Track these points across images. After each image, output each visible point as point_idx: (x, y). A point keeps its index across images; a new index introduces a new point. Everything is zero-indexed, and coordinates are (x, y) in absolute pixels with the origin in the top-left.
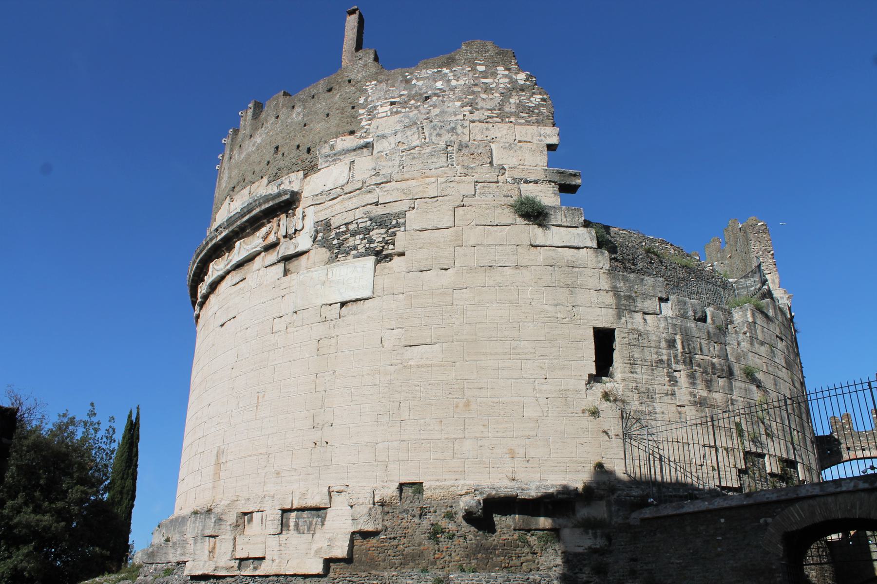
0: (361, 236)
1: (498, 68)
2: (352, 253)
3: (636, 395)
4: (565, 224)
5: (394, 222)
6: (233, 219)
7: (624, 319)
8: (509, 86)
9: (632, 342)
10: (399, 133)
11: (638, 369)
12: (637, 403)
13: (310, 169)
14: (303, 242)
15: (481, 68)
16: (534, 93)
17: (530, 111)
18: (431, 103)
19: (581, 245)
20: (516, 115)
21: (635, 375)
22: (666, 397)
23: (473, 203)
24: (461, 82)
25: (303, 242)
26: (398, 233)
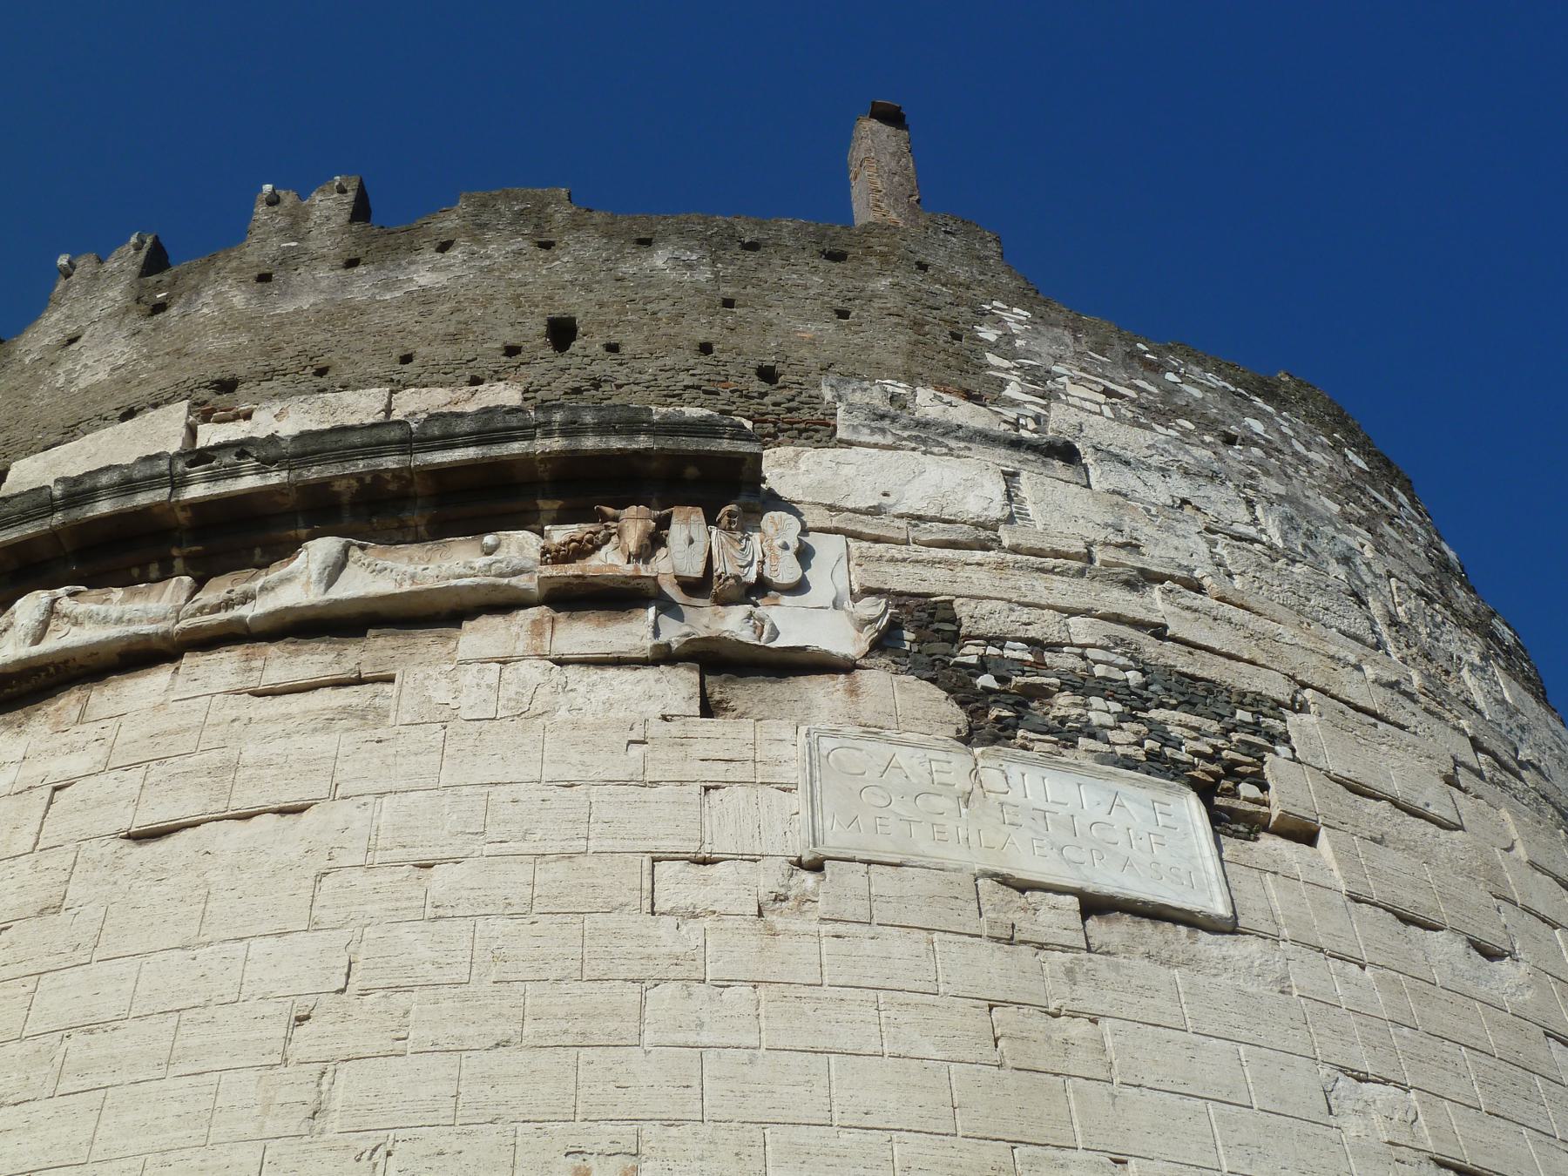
6: (356, 439)
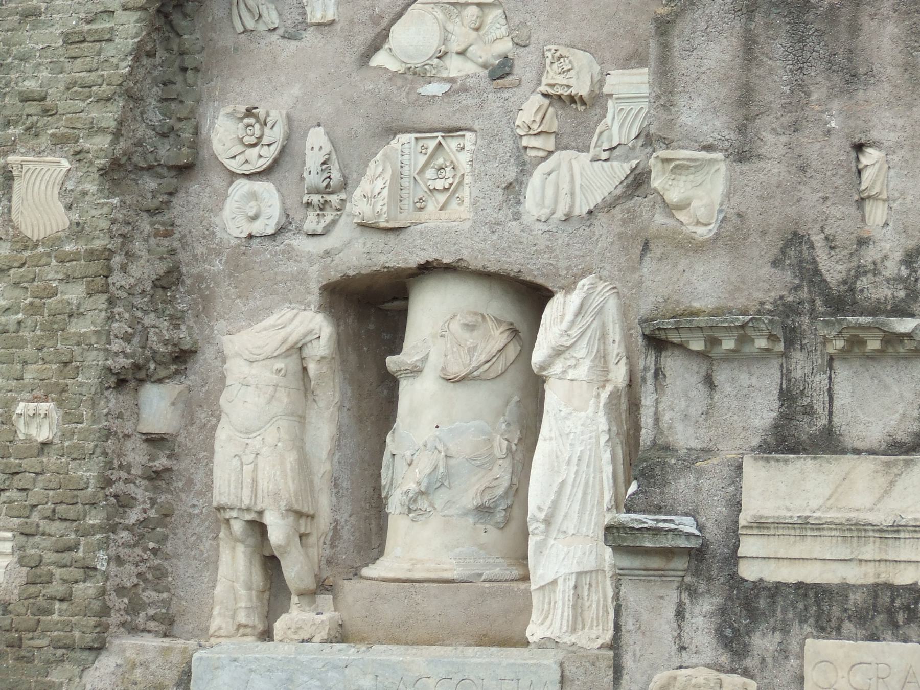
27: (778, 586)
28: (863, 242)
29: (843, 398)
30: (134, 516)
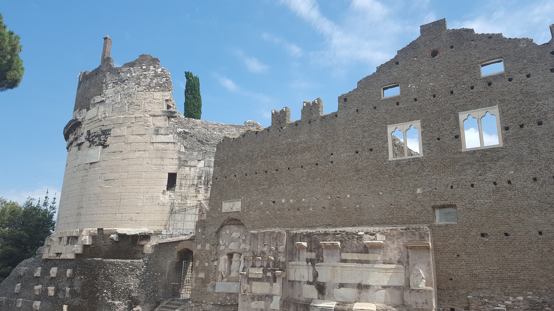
0: (98, 138)
1: (151, 67)
2: (95, 144)
3: (180, 197)
4: (164, 134)
5: (108, 133)
7: (181, 169)
8: (154, 75)
9: (183, 178)
10: (113, 96)
11: (183, 188)
12: (180, 200)
13: (88, 109)
14: (82, 139)
15: (144, 67)
16: (164, 77)
17: (160, 86)
18: (125, 83)
19: (169, 141)
20: (154, 87)
21: (181, 190)
22: (193, 198)
23: (133, 126)
24: (136, 74)
25: (82, 139)
26: (108, 137)
27: (251, 278)
28: (258, 252)
29: (256, 263)
30: (213, 272)
